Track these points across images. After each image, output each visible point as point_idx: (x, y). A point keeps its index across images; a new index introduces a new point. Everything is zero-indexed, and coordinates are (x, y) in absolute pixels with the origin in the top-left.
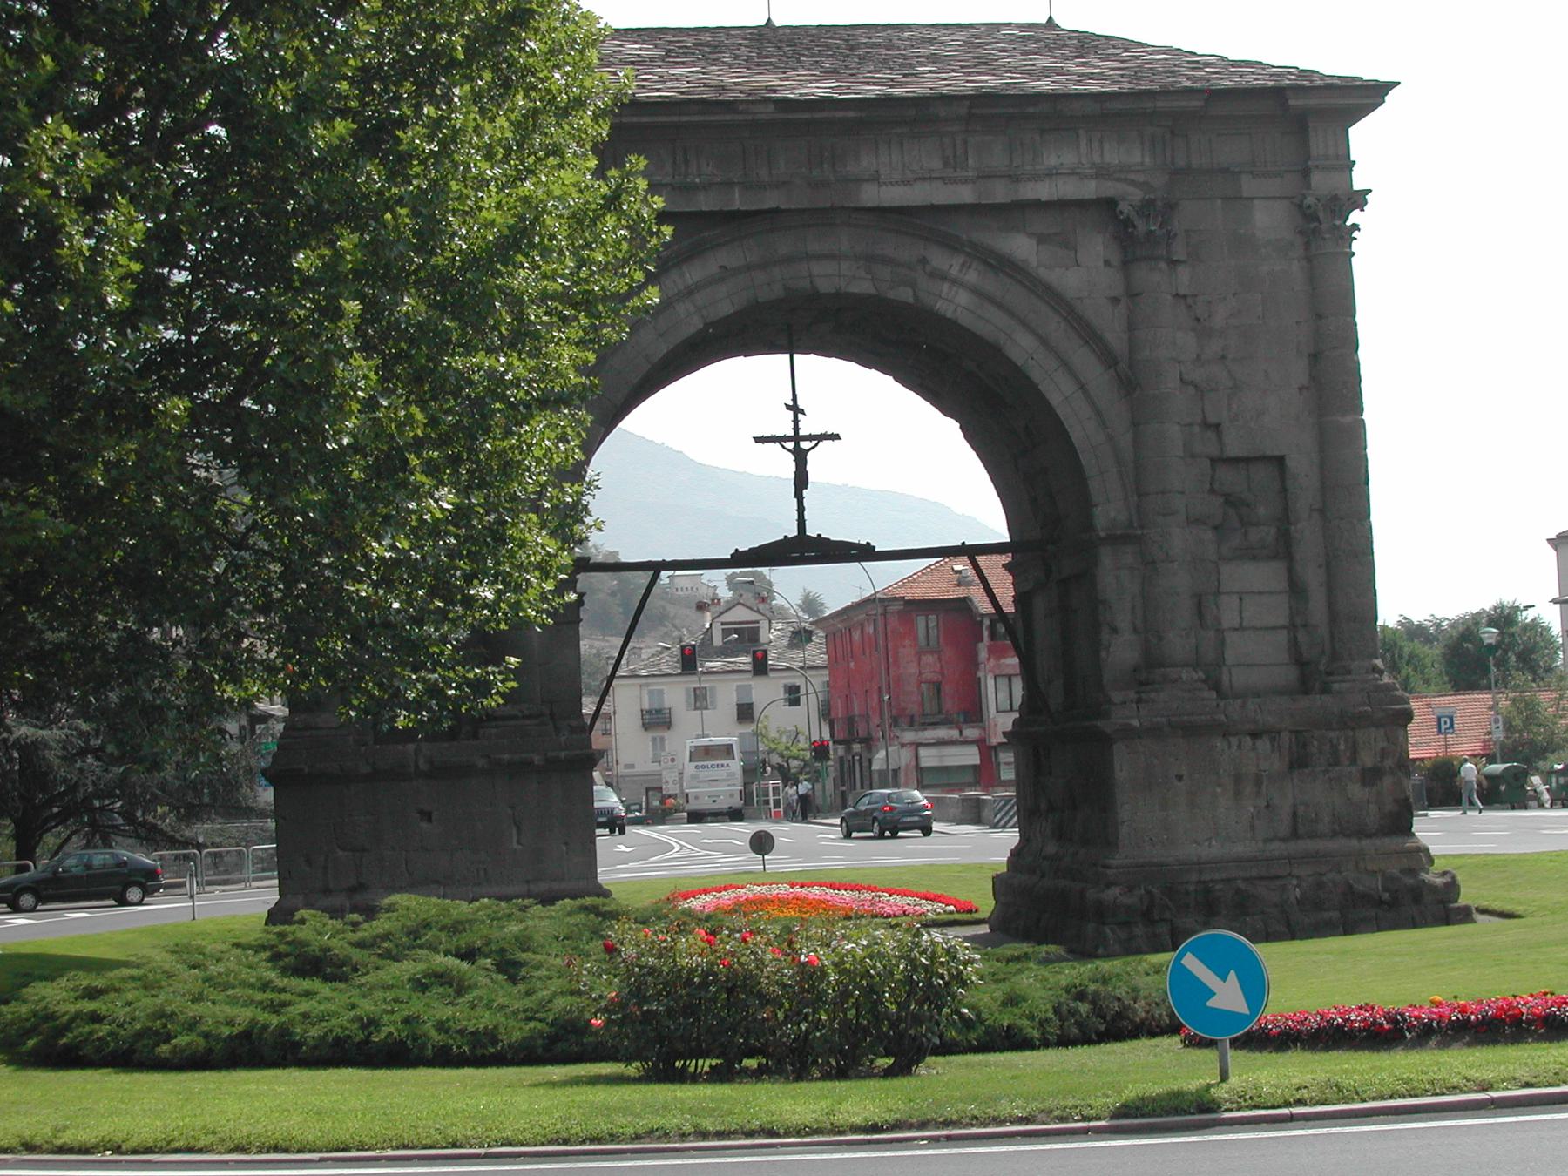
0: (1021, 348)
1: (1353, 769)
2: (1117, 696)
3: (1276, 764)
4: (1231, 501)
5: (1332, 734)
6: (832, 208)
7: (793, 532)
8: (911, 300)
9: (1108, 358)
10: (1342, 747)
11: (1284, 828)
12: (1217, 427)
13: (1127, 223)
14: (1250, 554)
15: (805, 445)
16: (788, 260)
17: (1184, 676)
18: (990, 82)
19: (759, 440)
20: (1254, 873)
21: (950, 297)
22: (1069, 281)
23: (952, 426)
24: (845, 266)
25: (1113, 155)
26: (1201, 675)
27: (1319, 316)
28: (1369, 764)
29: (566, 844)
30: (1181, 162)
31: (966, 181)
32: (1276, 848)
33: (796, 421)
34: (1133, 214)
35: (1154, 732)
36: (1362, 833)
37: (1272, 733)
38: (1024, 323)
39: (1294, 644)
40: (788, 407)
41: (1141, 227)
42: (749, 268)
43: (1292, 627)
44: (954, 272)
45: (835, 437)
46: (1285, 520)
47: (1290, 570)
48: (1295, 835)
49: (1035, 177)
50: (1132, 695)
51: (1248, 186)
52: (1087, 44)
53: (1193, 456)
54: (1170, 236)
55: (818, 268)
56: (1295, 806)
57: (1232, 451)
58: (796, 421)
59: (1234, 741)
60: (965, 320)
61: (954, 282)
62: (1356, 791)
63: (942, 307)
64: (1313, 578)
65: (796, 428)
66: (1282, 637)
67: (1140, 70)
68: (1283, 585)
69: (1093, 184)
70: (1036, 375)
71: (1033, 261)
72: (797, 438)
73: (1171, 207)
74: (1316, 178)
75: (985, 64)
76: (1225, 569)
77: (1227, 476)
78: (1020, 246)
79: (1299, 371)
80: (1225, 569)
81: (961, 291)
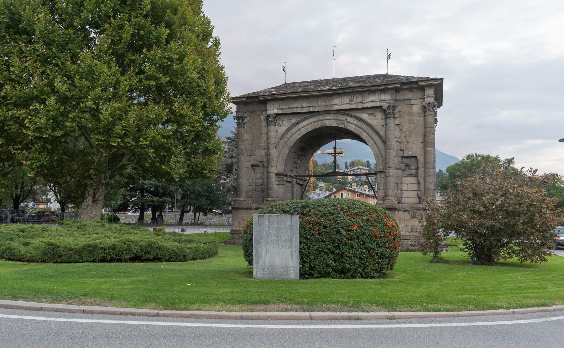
4: (407, 165)
5: (421, 212)
6: (328, 110)
7: (333, 171)
9: (380, 137)
10: (423, 215)
11: (410, 230)
12: (403, 150)
13: (385, 110)
14: (410, 175)
16: (321, 120)
19: (328, 154)
25: (384, 97)
26: (396, 199)
27: (426, 128)
30: (398, 98)
31: (353, 104)
32: (408, 234)
33: (335, 150)
34: (386, 108)
37: (408, 211)
39: (418, 195)
41: (388, 111)
42: (315, 122)
43: (417, 191)
44: (352, 121)
46: (417, 169)
48: (412, 231)
49: (367, 102)
51: (412, 102)
53: (398, 156)
54: (394, 113)
55: (327, 121)
57: (406, 155)
58: (335, 150)
59: (400, 212)
60: (353, 130)
61: (352, 123)
63: (350, 128)
64: (422, 180)
66: (416, 192)
68: (416, 182)
71: (367, 119)
73: (394, 107)
74: (426, 99)
77: (405, 160)
78: (364, 116)
79: (421, 139)
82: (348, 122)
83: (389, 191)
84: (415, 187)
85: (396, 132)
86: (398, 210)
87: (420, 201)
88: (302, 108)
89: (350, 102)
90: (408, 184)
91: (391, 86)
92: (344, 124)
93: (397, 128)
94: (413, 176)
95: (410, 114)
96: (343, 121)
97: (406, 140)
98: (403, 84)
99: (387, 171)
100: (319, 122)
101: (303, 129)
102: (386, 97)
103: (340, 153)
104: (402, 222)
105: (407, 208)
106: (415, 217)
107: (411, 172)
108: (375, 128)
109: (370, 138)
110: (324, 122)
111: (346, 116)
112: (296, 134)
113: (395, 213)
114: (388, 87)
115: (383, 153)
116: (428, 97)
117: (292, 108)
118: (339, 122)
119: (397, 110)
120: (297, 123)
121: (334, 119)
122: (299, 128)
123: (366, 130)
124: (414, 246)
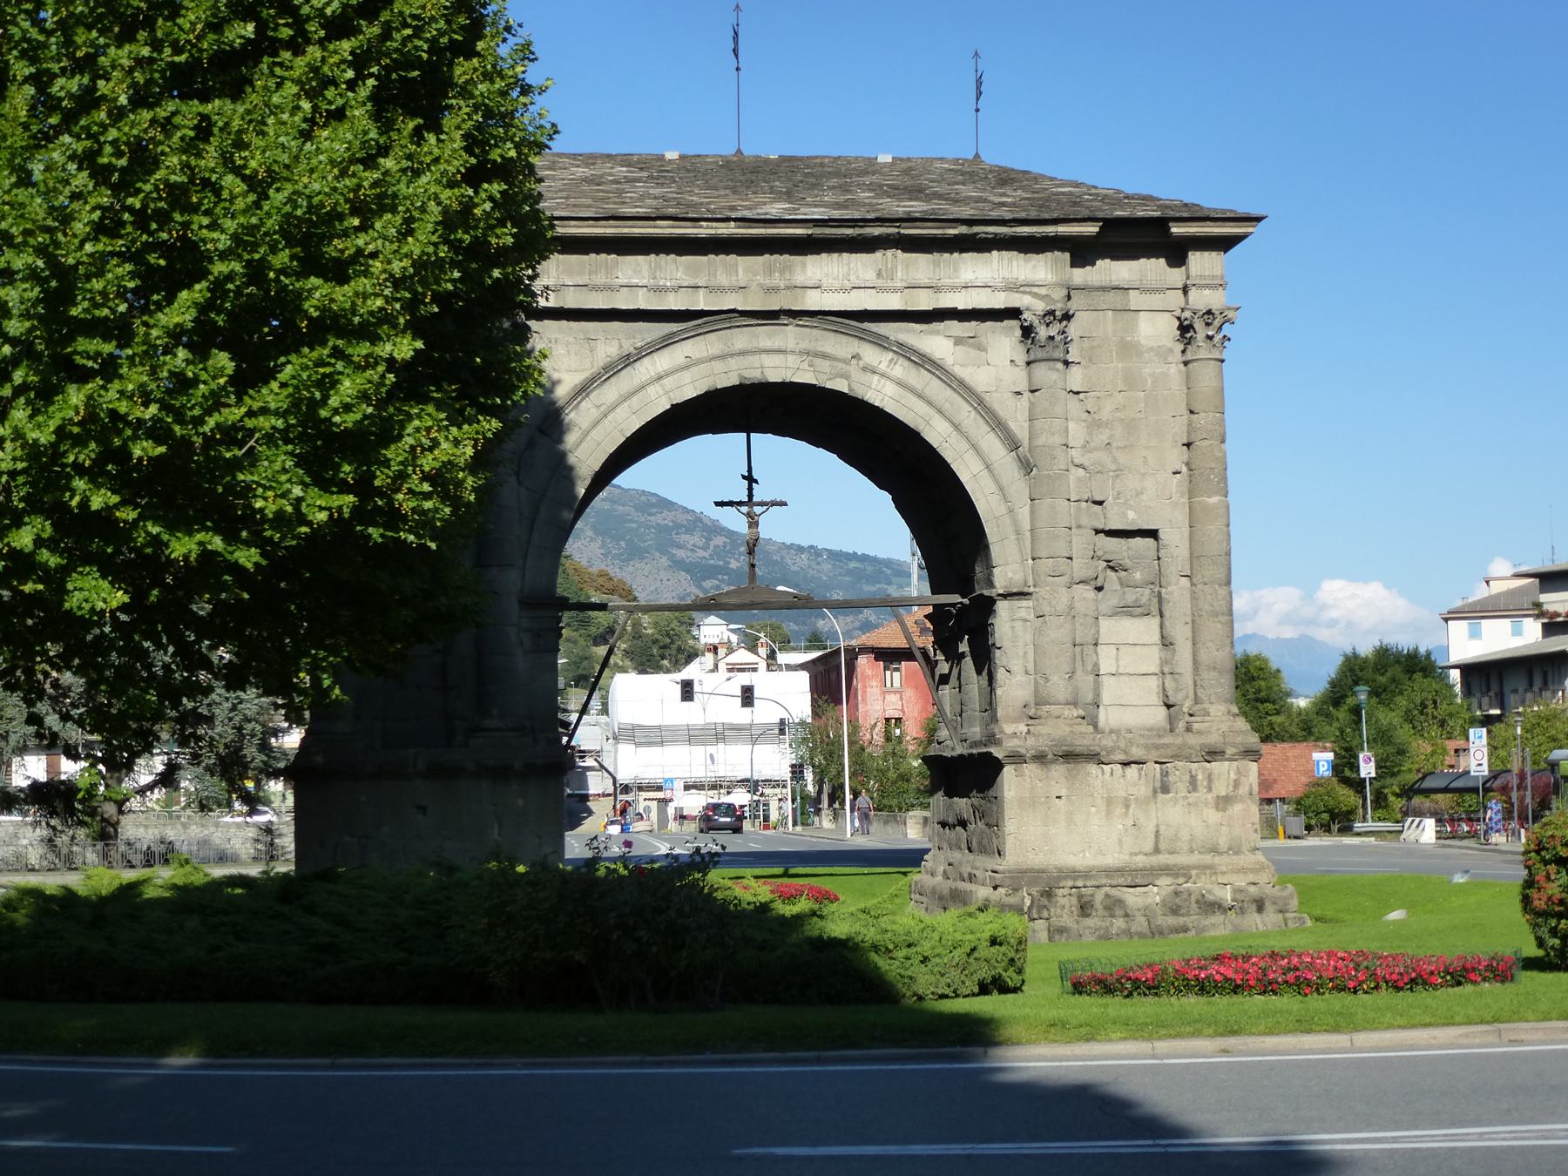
0: (937, 434)
1: (1210, 796)
2: (1009, 729)
3: (1143, 790)
8: (846, 390)
9: (1013, 445)
11: (1149, 846)
14: (1127, 610)
15: (758, 510)
16: (743, 353)
17: (1066, 713)
18: (917, 207)
20: (1121, 881)
21: (879, 388)
22: (979, 378)
23: (887, 497)
24: (791, 358)
26: (1082, 713)
28: (1223, 794)
29: (540, 837)
31: (895, 290)
32: (1141, 861)
33: (750, 489)
35: (1040, 758)
36: (1215, 850)
38: (940, 411)
40: (744, 477)
41: (1042, 332)
44: (883, 367)
45: (783, 504)
46: (1157, 581)
47: (1162, 626)
50: (1023, 728)
51: (1135, 300)
52: (1005, 178)
55: (768, 360)
56: (1157, 826)
58: (750, 489)
59: (1107, 768)
60: (890, 408)
61: (883, 375)
62: (1213, 816)
65: (750, 495)
66: (1153, 683)
67: (1048, 199)
68: (1156, 638)
69: (1002, 295)
70: (948, 456)
72: (750, 501)
75: (916, 192)
76: (1105, 625)
79: (1177, 457)
80: (1105, 625)
81: (888, 383)
82: (865, 369)
83: (1055, 678)
84: (1151, 659)
85: (1072, 425)
86: (1095, 758)
87: (1171, 720)
88: (659, 290)
89: (880, 283)
90: (1123, 649)
91: (1062, 229)
92: (846, 376)
93: (1073, 403)
94: (1139, 610)
95: (1128, 349)
96: (845, 361)
97: (1115, 460)
98: (1109, 224)
99: (1042, 592)
100: (733, 363)
101: (652, 390)
102: (1042, 270)
103: (774, 504)
104: (1119, 810)
105: (1137, 753)
106: (1165, 789)
107: (1130, 596)
108: (987, 397)
109: (964, 445)
110: (755, 360)
111: (856, 342)
112: (621, 411)
113: (1088, 774)
114: (1050, 230)
115: (1024, 513)
116: (1201, 287)
117: (609, 288)
118: (825, 365)
119: (1074, 329)
120: (628, 361)
121: (801, 353)
122: (637, 382)
123: (946, 407)
124: (1175, 911)
